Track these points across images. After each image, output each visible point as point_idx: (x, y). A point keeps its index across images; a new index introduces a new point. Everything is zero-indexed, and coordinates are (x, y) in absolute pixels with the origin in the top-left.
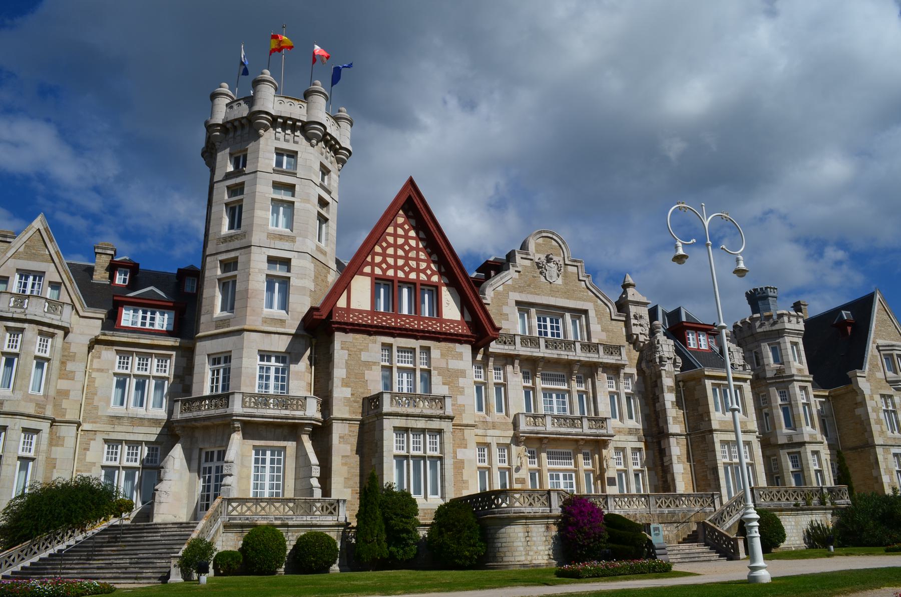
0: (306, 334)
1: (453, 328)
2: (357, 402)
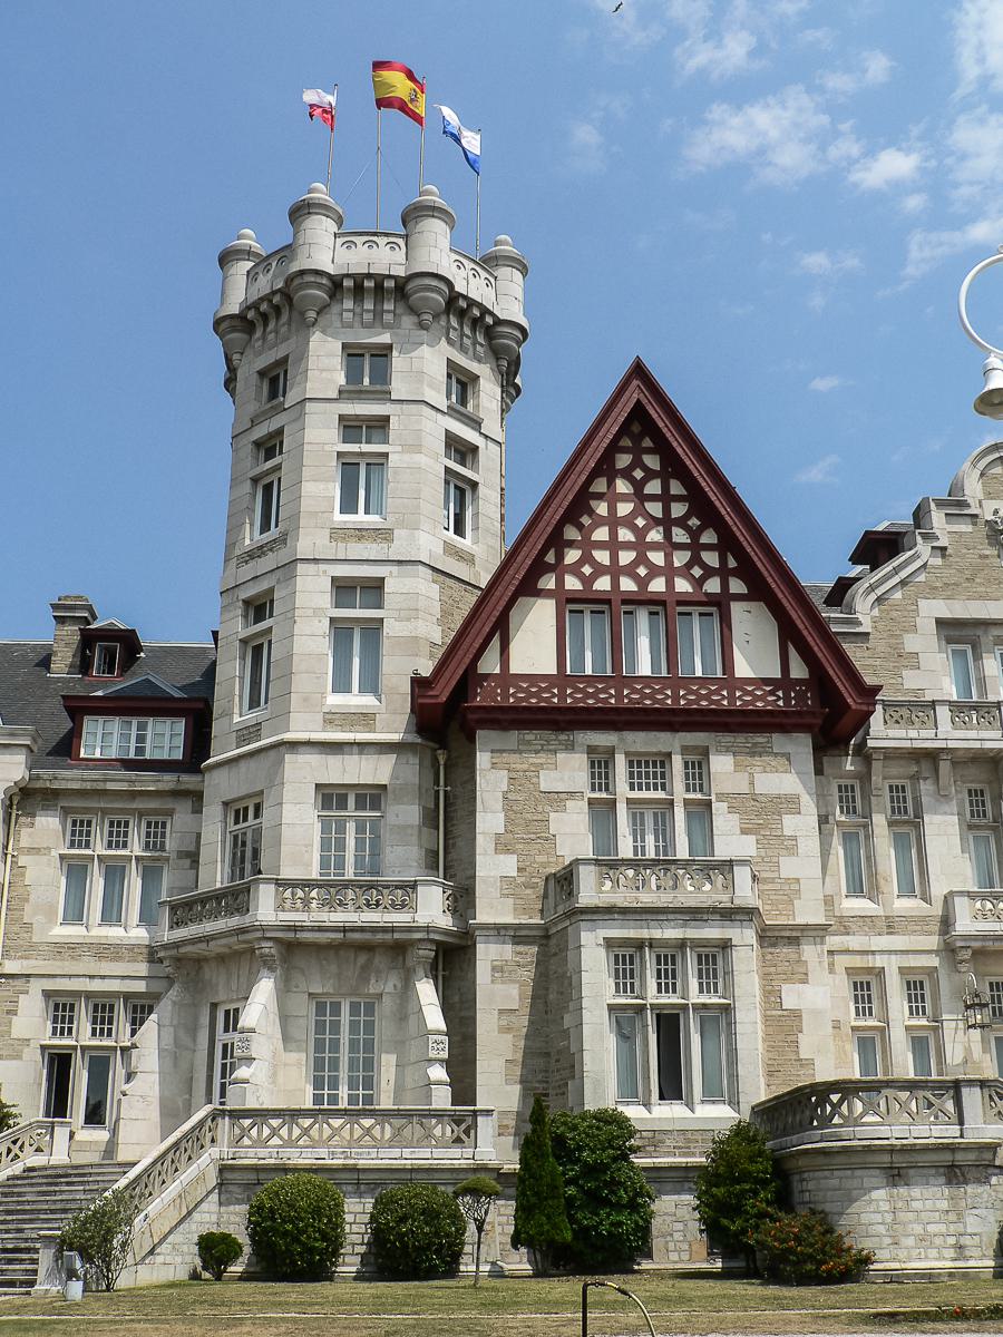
0: (419, 741)
2: (534, 886)
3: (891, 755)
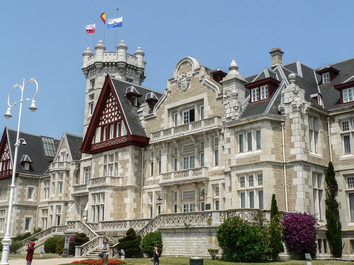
1: (124, 140)
3: (155, 145)
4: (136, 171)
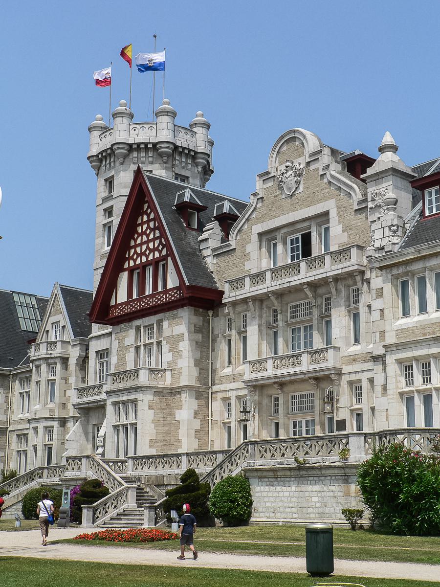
1: (173, 296)
3: (234, 304)
4: (198, 355)
